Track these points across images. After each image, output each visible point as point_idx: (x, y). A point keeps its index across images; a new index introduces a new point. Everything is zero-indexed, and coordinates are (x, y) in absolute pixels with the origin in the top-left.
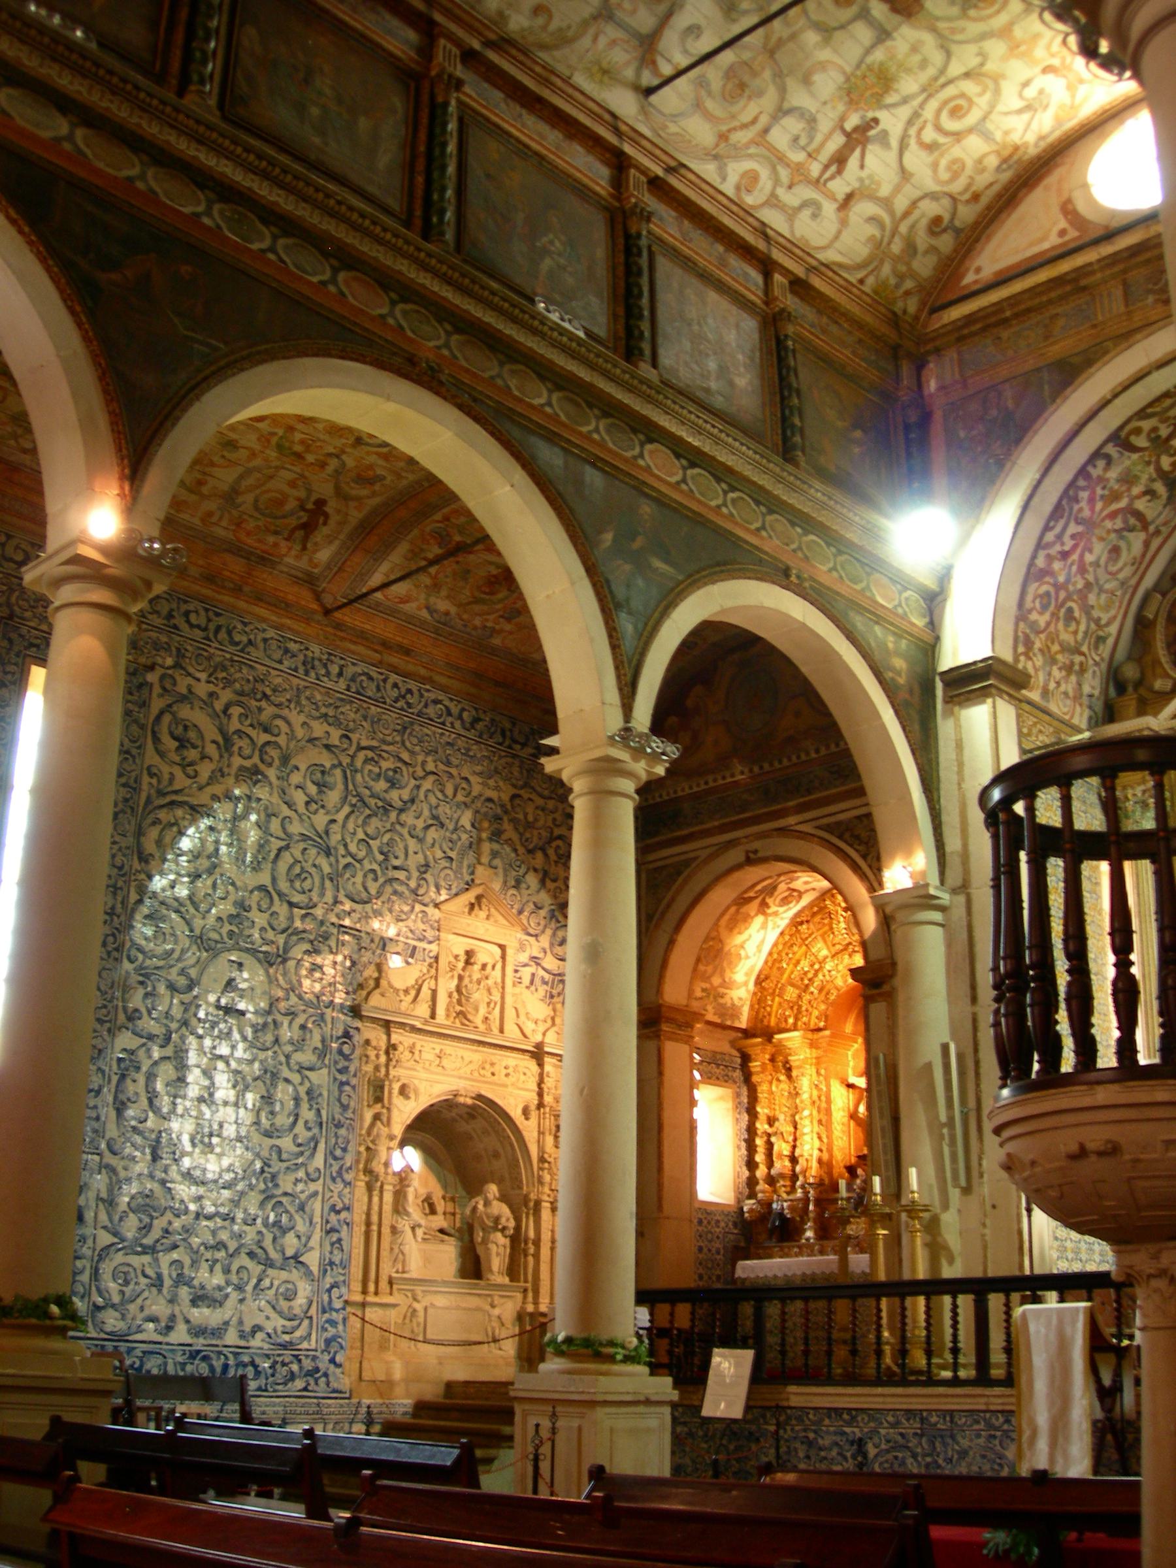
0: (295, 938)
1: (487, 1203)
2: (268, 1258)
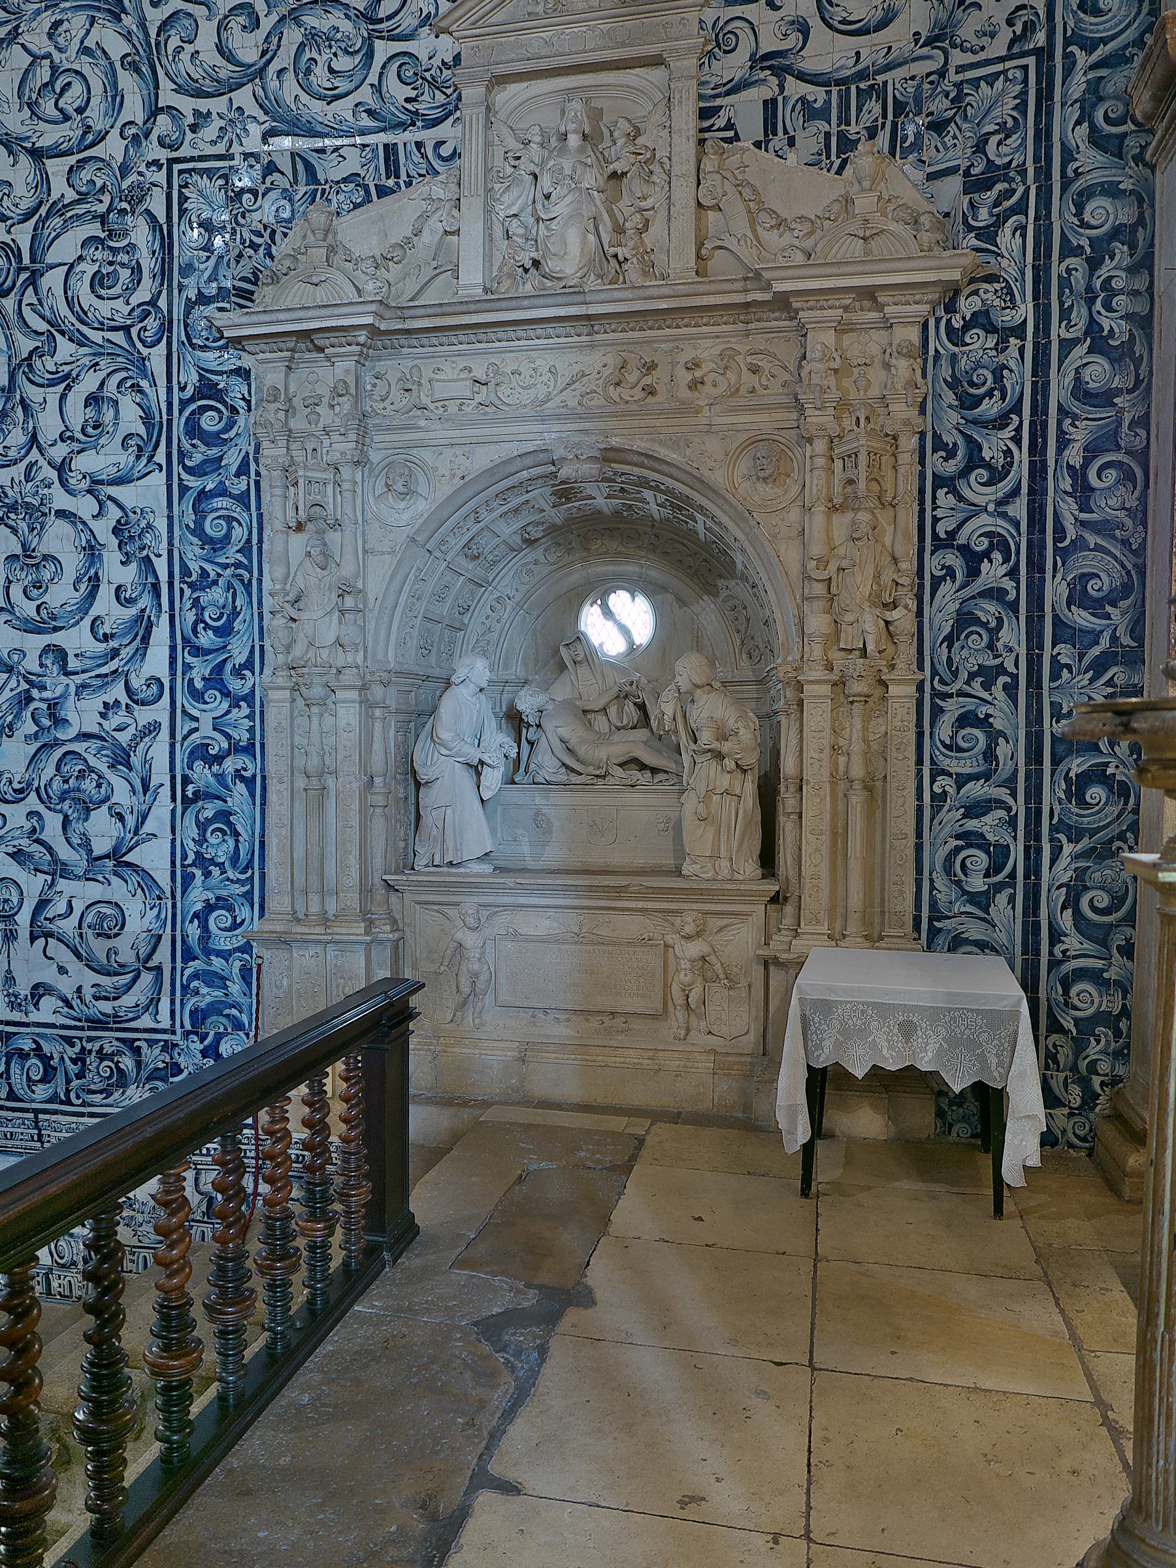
0: (57, 222)
2: (55, 859)
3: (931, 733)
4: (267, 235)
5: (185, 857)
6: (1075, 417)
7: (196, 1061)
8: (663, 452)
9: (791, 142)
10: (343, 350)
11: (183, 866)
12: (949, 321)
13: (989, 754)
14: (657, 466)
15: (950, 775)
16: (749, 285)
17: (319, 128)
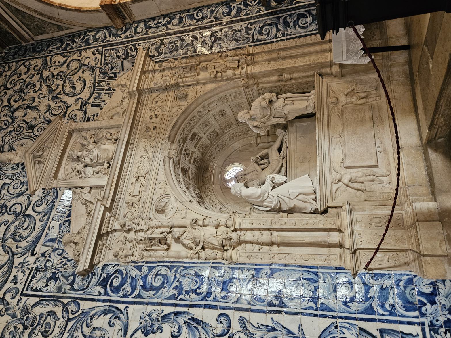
1: (252, 119)
3: (264, 41)
4: (63, 260)
5: (311, 308)
6: (185, 24)
7: (439, 308)
8: (173, 122)
9: (104, 101)
10: (110, 224)
11: (317, 310)
12: (156, 56)
13: (270, 25)
14: (177, 126)
15: (276, 33)
16: (133, 98)
17: (40, 234)
